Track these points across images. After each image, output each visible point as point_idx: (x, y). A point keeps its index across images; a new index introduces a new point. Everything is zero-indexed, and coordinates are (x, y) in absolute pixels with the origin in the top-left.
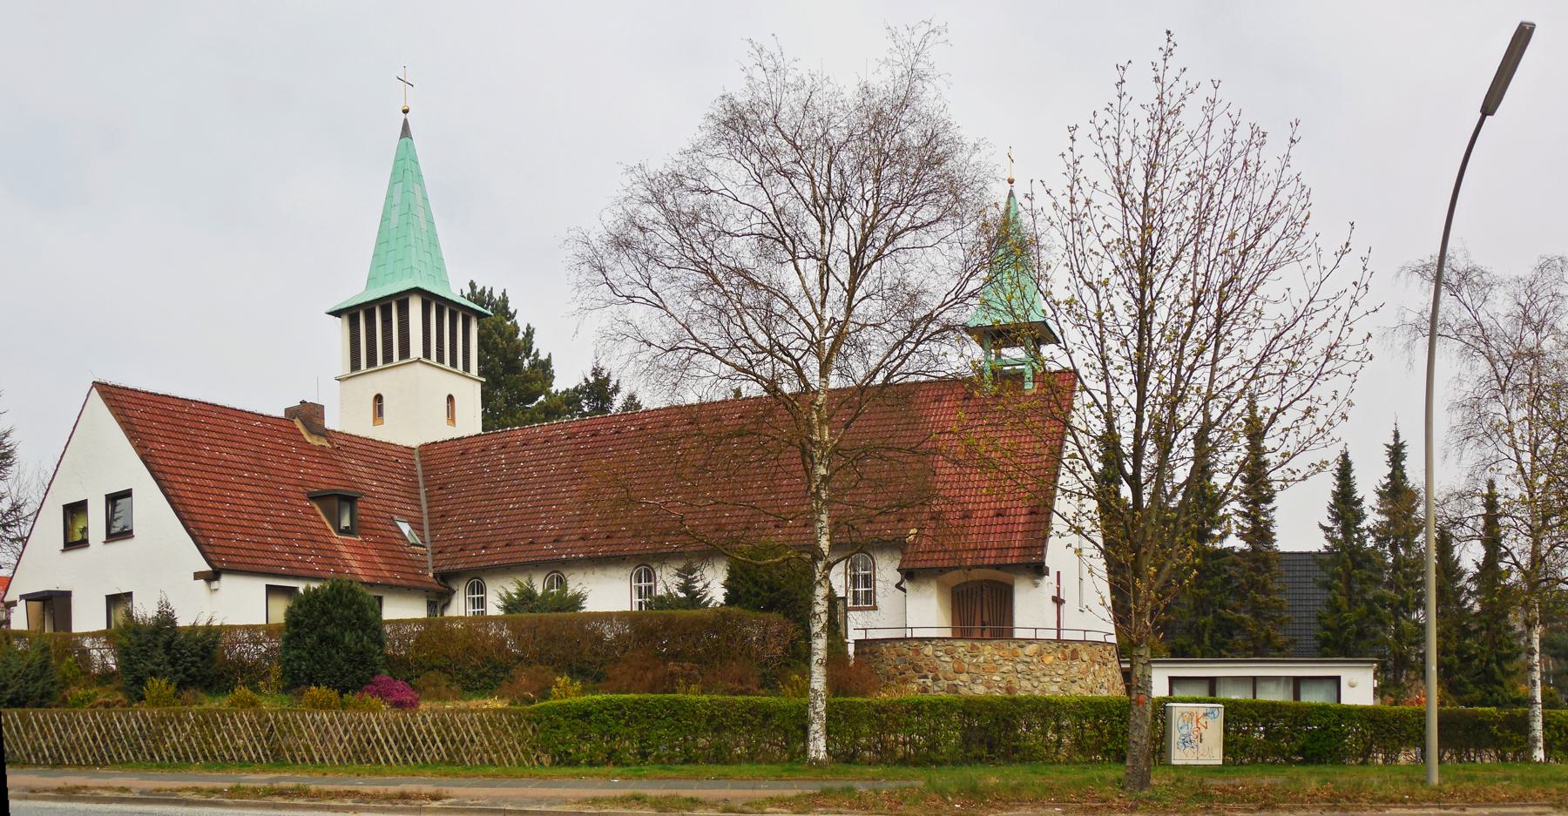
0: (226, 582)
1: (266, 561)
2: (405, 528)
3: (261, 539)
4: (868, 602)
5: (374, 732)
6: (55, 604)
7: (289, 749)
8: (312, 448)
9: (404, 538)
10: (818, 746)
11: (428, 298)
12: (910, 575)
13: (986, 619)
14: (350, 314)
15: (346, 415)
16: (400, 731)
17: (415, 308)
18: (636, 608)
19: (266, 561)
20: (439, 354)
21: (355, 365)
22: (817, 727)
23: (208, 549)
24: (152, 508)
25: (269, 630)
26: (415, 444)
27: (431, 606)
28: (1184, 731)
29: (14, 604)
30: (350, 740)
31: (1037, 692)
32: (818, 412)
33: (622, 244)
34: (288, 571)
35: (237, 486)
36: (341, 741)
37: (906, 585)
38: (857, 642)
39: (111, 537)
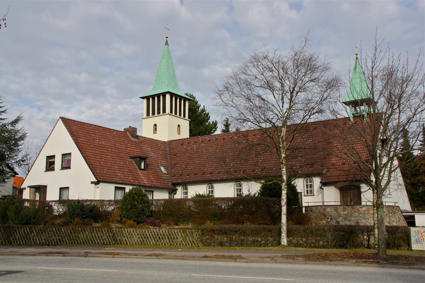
0: (101, 184)
1: (115, 179)
2: (163, 169)
3: (114, 171)
4: (310, 193)
5: (146, 235)
6: (41, 189)
7: (120, 240)
8: (132, 142)
9: (162, 172)
10: (284, 241)
11: (172, 95)
12: (324, 184)
13: (352, 198)
14: (147, 98)
15: (145, 131)
16: (155, 235)
17: (168, 97)
18: (236, 196)
19: (115, 179)
20: (174, 112)
21: (148, 114)
22: (284, 234)
23: (96, 174)
24: (78, 159)
25: (116, 202)
26: (166, 141)
27: (170, 193)
28: (416, 237)
29: (25, 189)
30: (139, 238)
31: (367, 224)
32: (282, 138)
33: (227, 88)
34: (123, 182)
35: (106, 154)
36: (136, 237)
37: (323, 187)
38: (305, 207)
39: (63, 168)
